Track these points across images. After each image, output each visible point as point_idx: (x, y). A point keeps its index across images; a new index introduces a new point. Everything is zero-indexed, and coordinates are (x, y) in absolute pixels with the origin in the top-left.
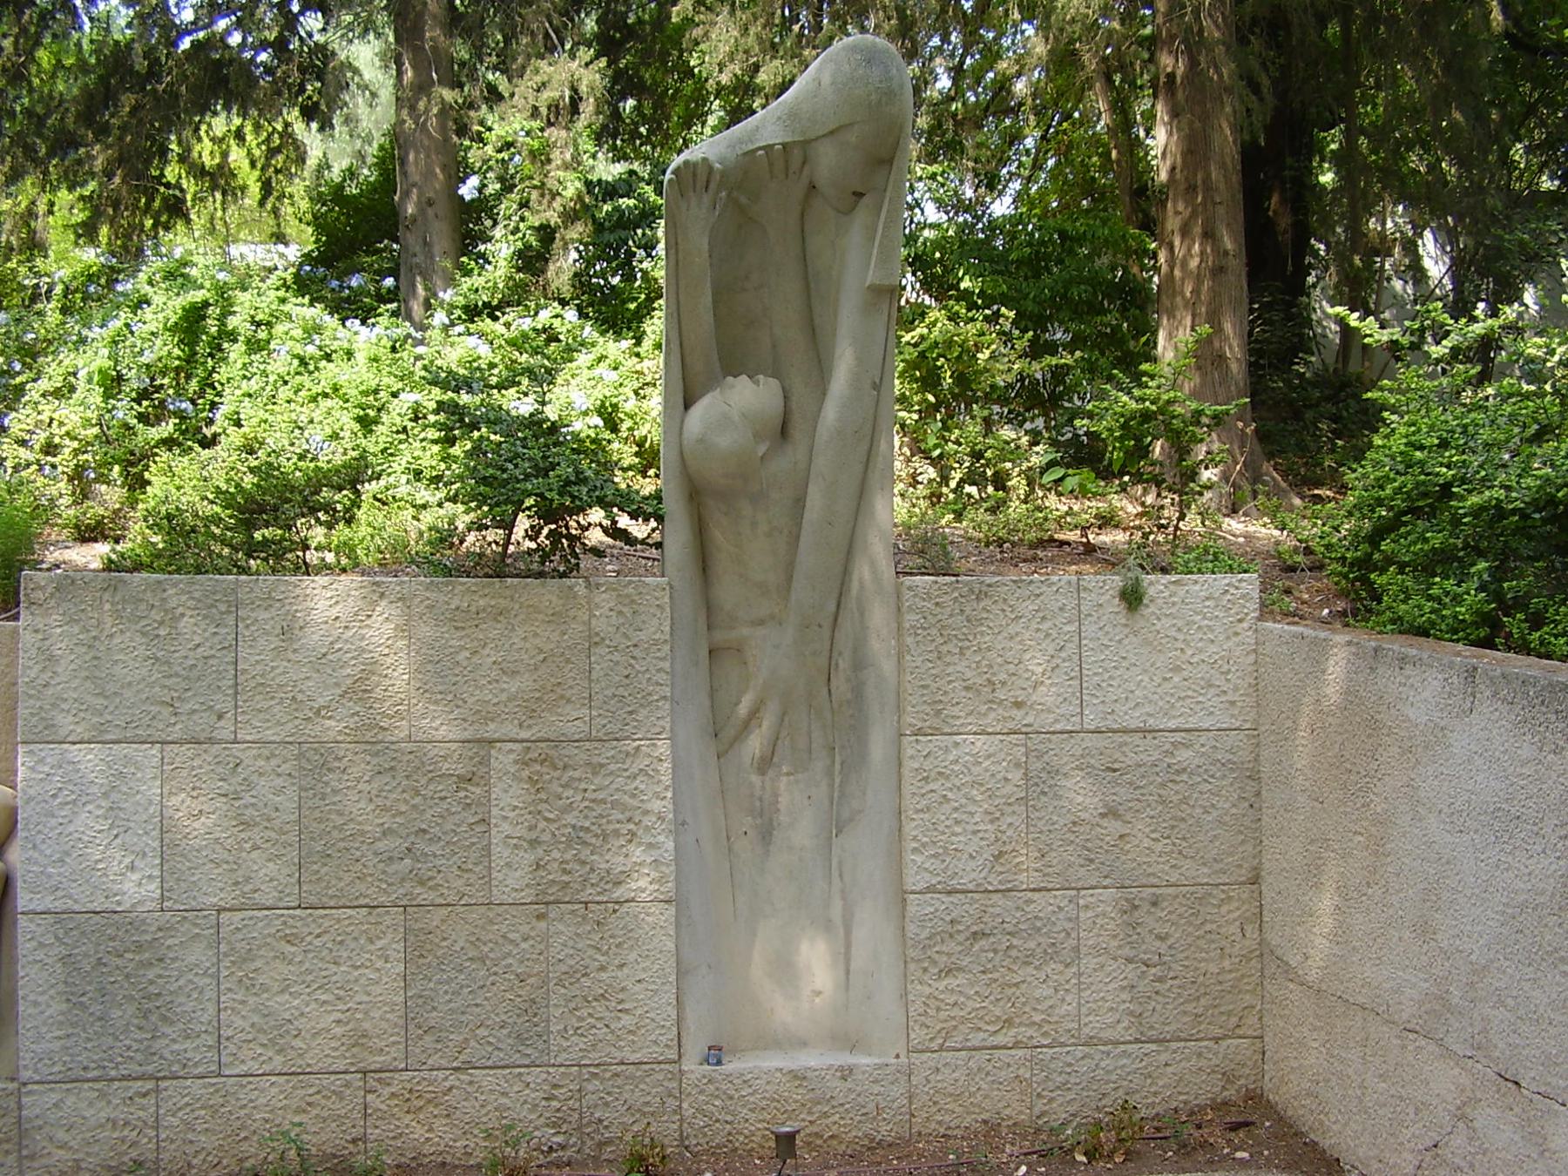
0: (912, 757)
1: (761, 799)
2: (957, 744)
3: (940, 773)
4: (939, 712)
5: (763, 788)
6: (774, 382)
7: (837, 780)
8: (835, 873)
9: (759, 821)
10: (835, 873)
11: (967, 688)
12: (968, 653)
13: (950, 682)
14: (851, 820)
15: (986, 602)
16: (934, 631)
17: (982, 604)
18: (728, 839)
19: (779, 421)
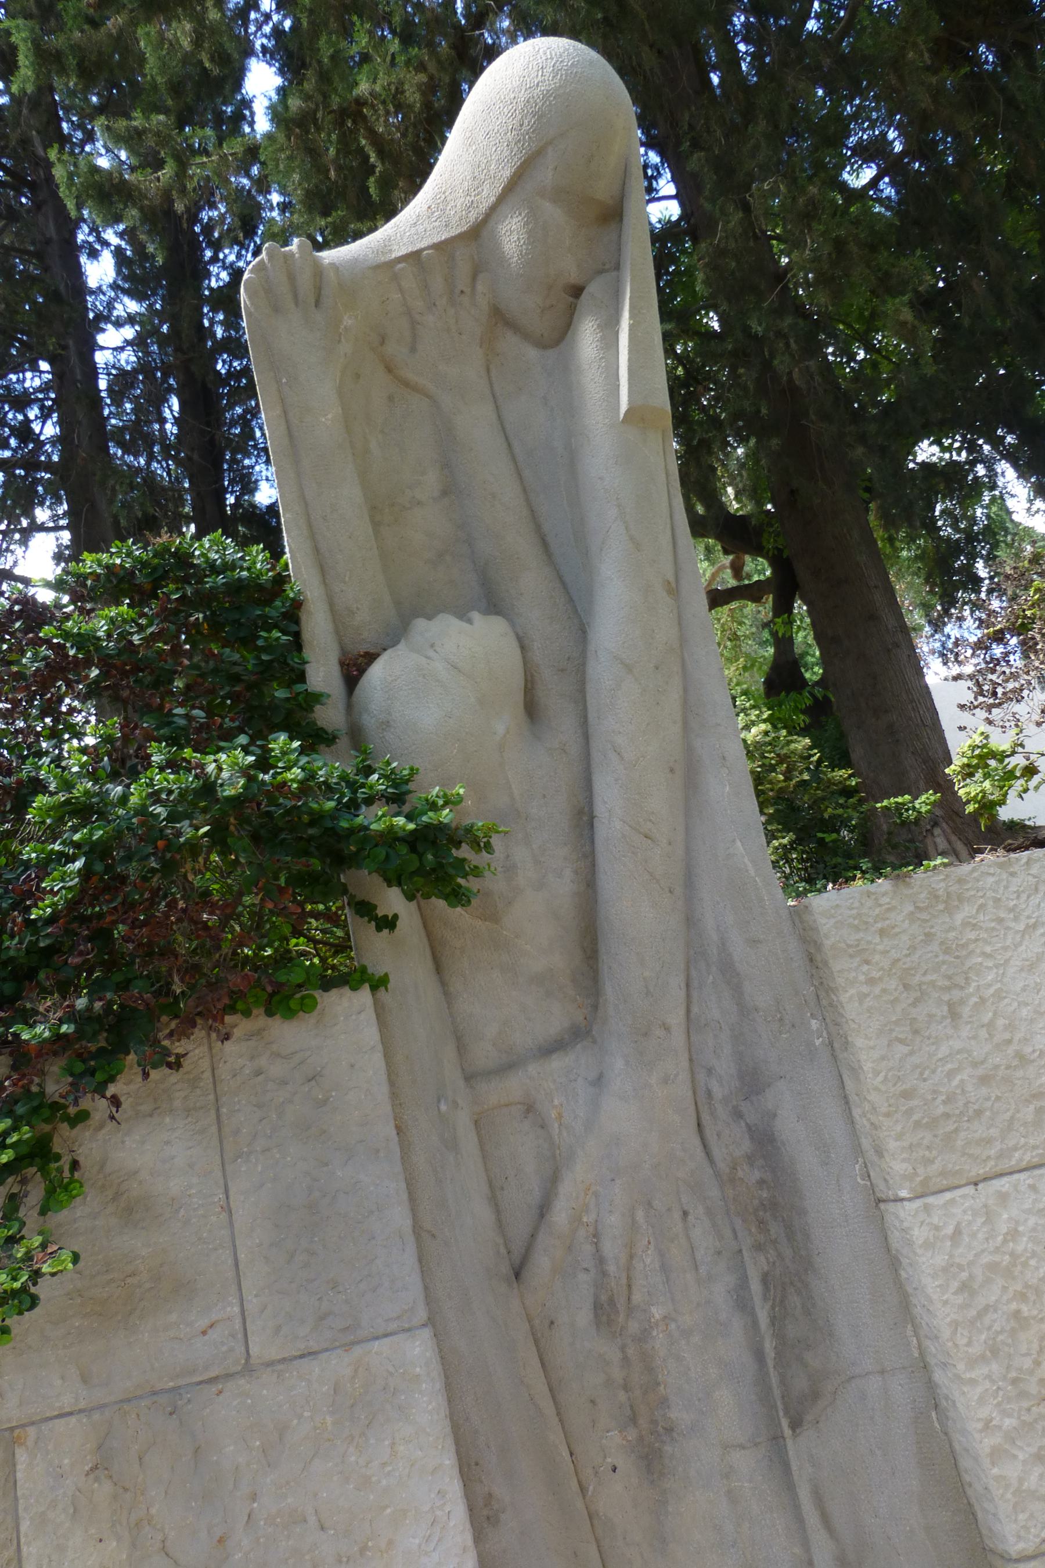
0: (928, 1245)
1: (626, 1388)
2: (1003, 1198)
3: (992, 1267)
4: (949, 1138)
5: (626, 1360)
6: (497, 626)
7: (763, 1317)
8: (812, 1519)
9: (632, 1434)
10: (812, 1519)
11: (984, 1080)
12: (966, 1011)
13: (950, 1074)
14: (815, 1395)
15: (966, 911)
16: (893, 984)
17: (959, 918)
18: (583, 1489)
19: (517, 680)
